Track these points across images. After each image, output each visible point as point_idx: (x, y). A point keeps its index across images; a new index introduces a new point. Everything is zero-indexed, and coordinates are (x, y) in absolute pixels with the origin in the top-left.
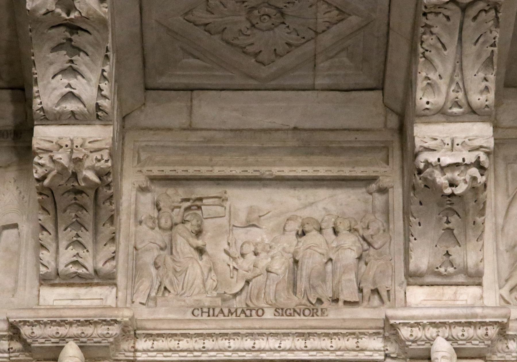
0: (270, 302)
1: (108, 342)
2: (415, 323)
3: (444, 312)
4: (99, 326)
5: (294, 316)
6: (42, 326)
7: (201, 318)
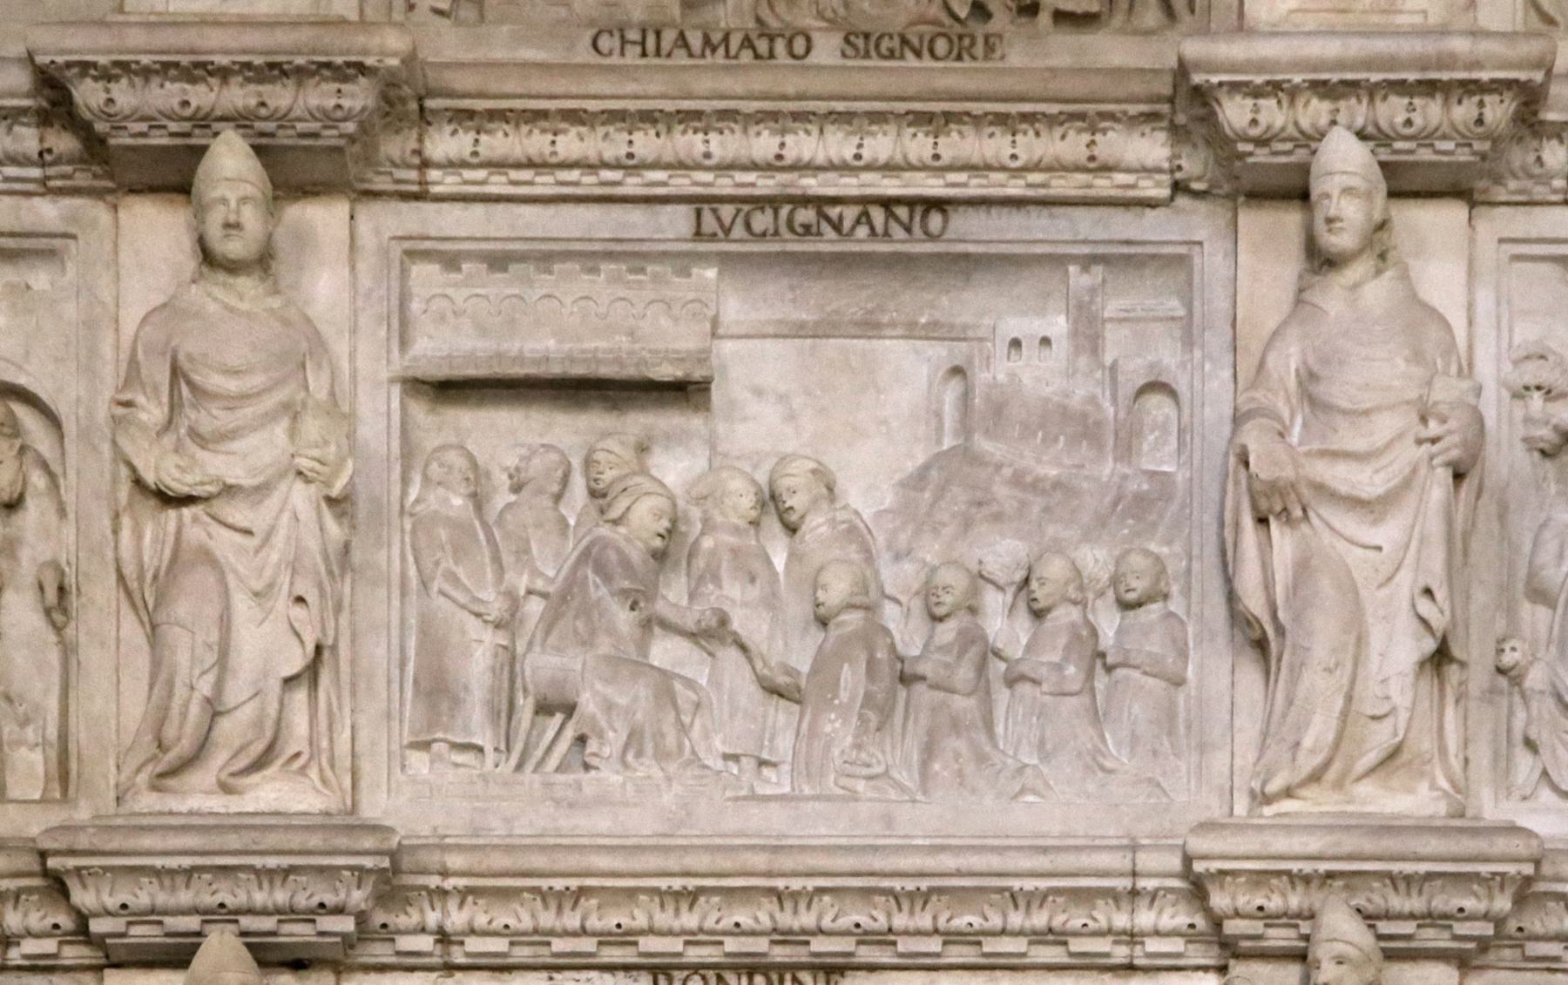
0: (829, 14)
1: (341, 136)
2: (1268, 83)
3: (1356, 48)
4: (313, 81)
5: (902, 57)
6: (138, 81)
7: (621, 61)
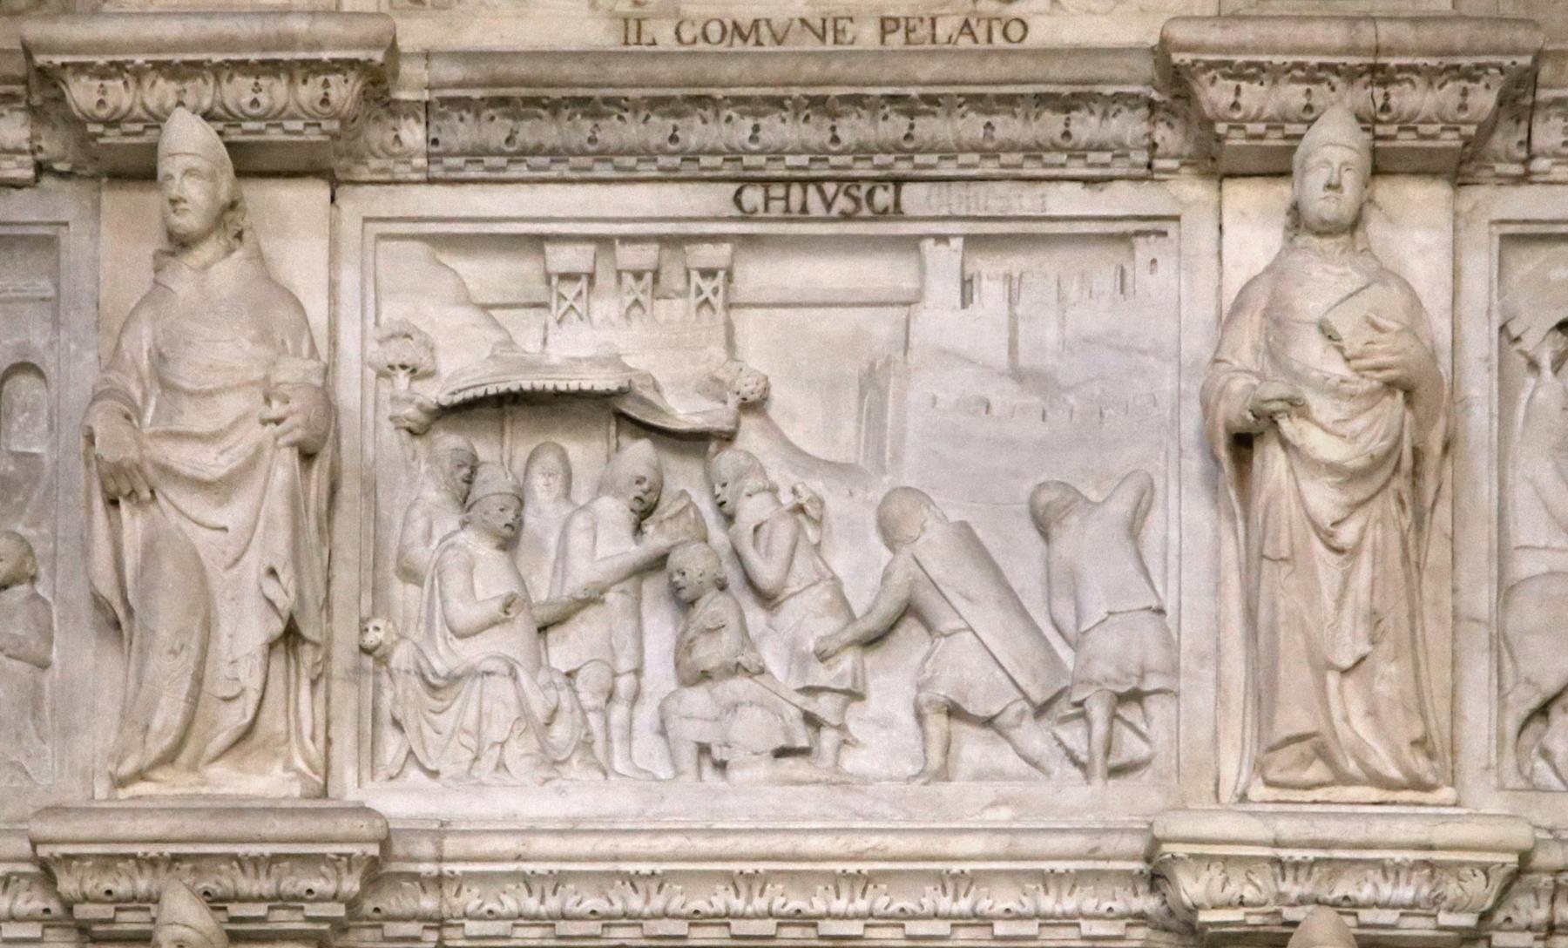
2: (112, 64)
